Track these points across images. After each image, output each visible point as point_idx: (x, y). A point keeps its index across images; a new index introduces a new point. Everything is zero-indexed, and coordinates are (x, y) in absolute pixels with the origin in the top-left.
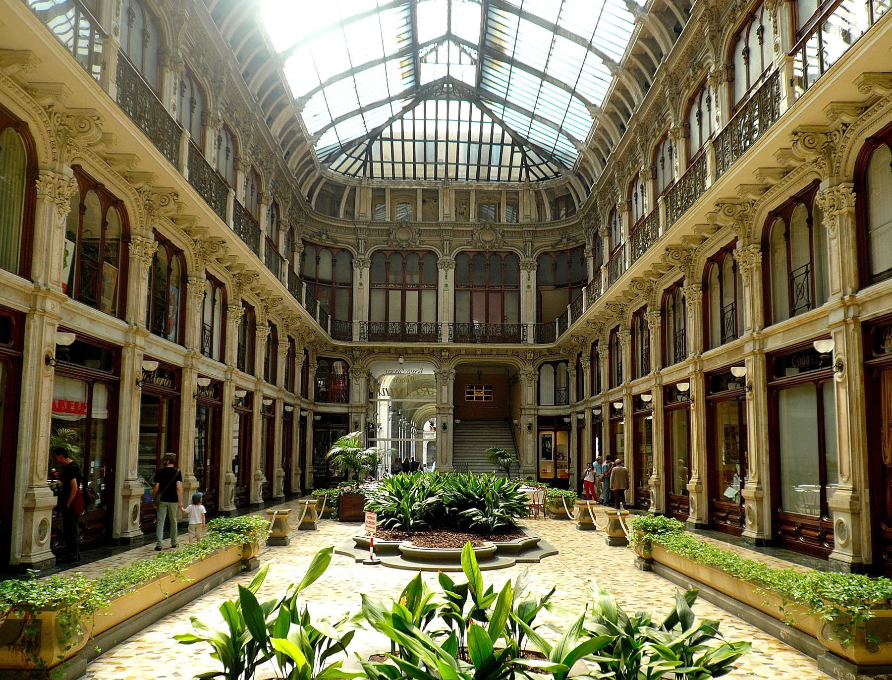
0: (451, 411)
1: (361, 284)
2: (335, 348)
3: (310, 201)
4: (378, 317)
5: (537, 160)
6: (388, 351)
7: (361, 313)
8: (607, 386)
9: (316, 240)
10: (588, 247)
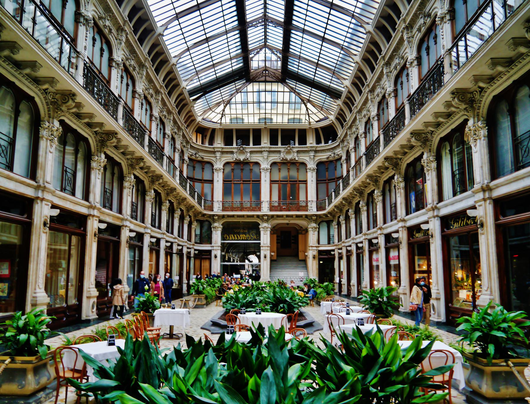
2: (204, 215)
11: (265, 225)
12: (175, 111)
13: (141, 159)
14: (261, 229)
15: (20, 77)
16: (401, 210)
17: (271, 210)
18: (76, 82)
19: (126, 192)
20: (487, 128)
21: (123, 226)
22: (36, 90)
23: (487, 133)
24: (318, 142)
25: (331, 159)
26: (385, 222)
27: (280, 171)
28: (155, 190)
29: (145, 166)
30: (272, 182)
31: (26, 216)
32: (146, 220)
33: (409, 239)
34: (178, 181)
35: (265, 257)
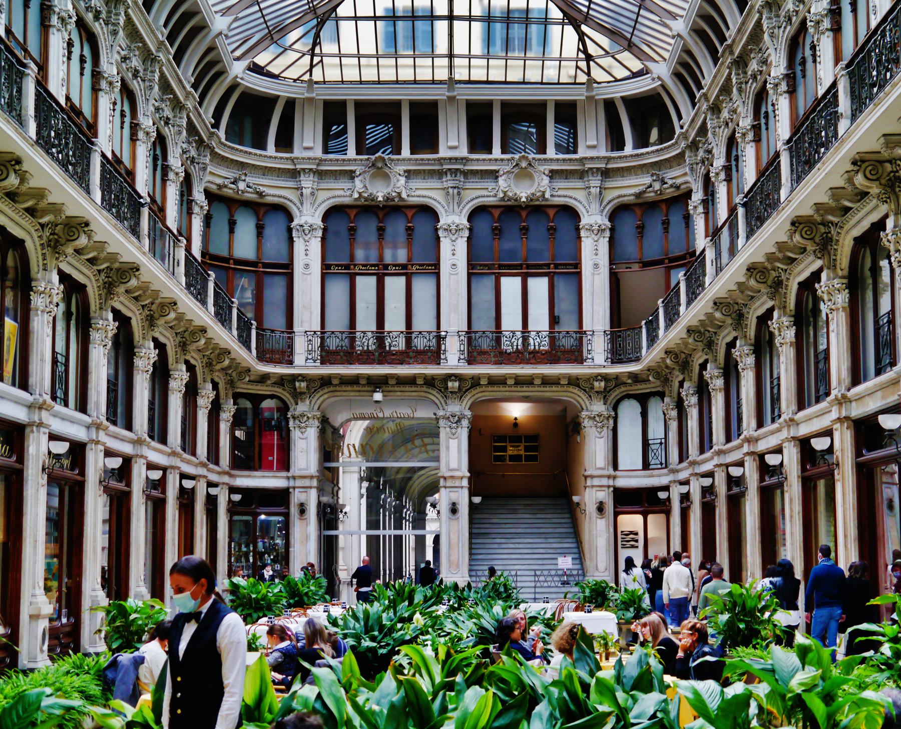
0: (465, 483)
1: (307, 266)
2: (264, 378)
3: (216, 125)
4: (337, 321)
6: (354, 381)
7: (307, 316)
9: (228, 192)
10: (697, 196)
12: (166, 56)
17: (471, 361)
19: (41, 326)
20: (847, 291)
23: (847, 300)
24: (617, 142)
28: (115, 312)
29: (102, 256)
35: (454, 510)
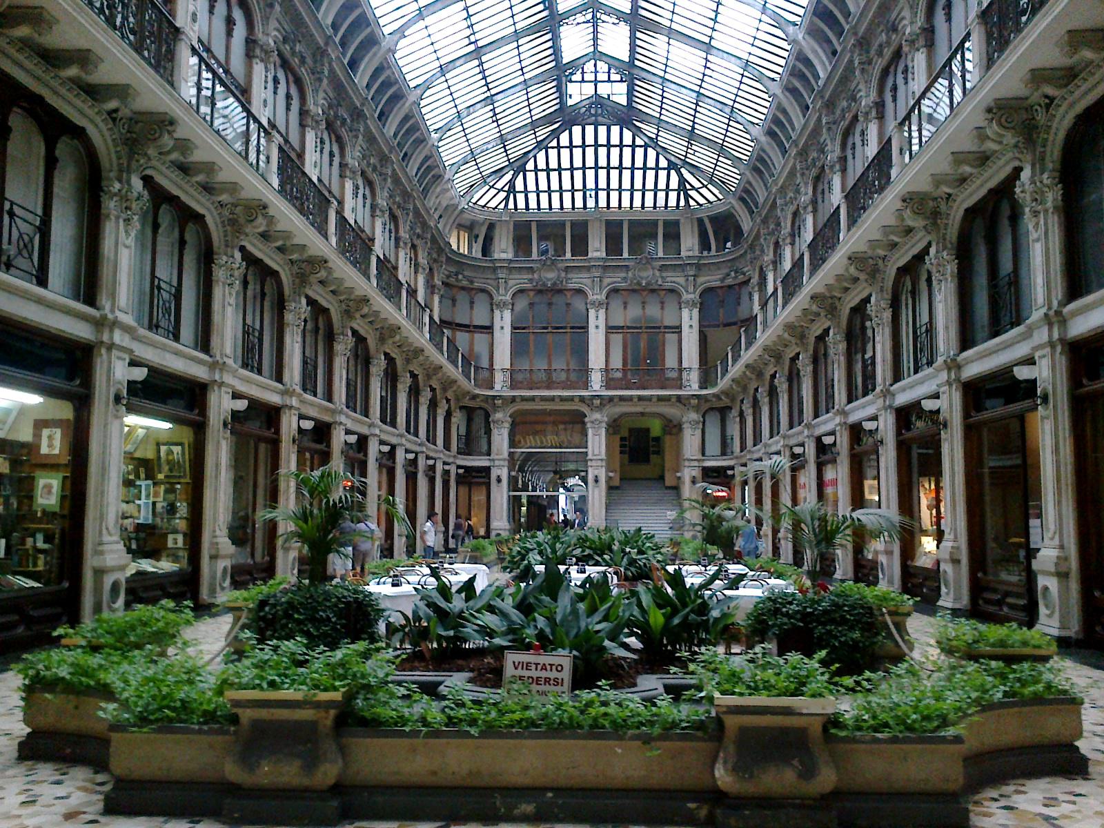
2: (474, 397)
5: (697, 185)
8: (768, 435)
11: (597, 416)
13: (365, 300)
14: (589, 425)
15: (187, 187)
16: (840, 394)
17: (608, 387)
18: (264, 185)
21: (335, 423)
22: (208, 204)
24: (705, 245)
25: (729, 281)
26: (816, 416)
27: (625, 308)
30: (610, 329)
31: (197, 411)
32: (371, 411)
33: (852, 448)
34: (428, 336)
35: (596, 481)
